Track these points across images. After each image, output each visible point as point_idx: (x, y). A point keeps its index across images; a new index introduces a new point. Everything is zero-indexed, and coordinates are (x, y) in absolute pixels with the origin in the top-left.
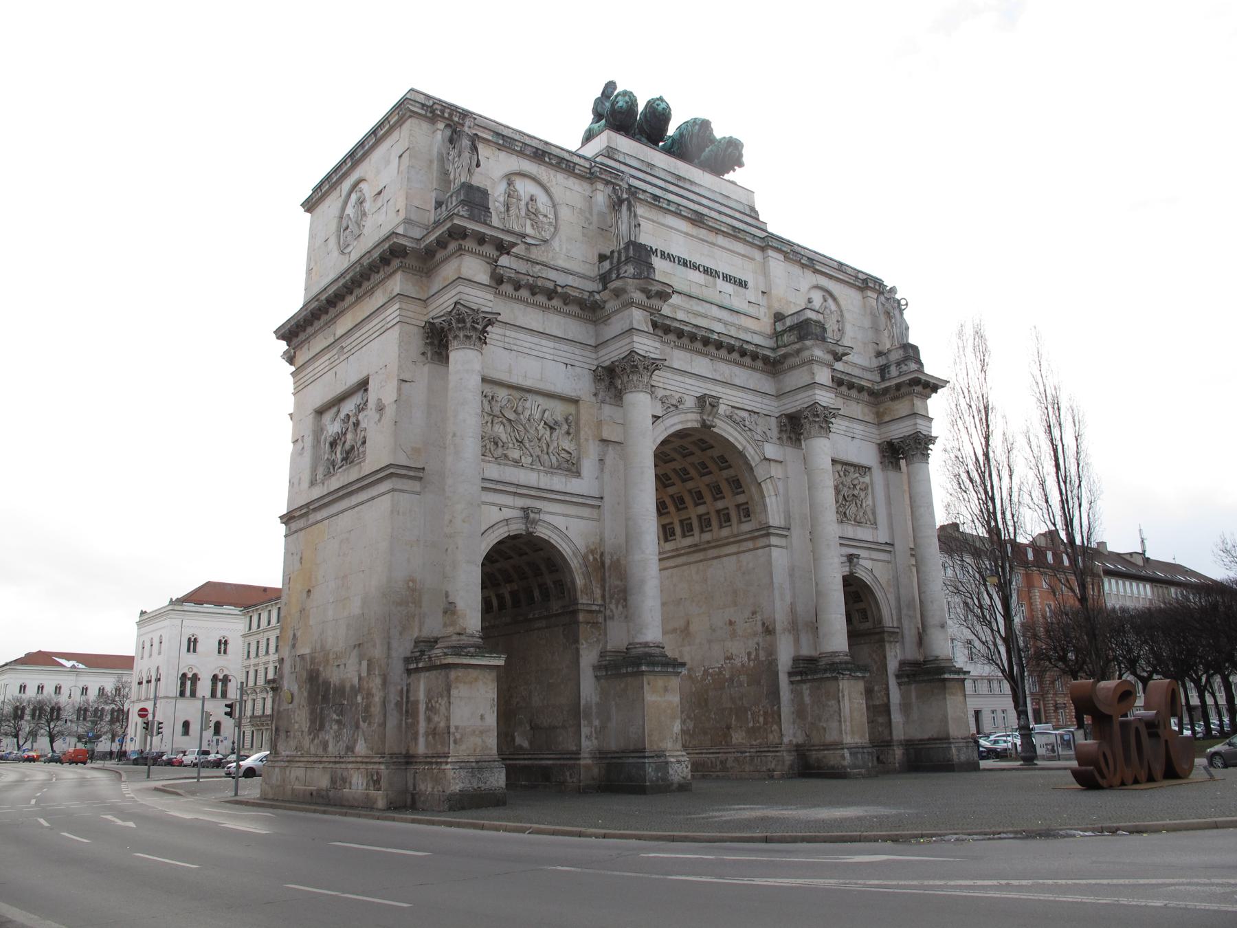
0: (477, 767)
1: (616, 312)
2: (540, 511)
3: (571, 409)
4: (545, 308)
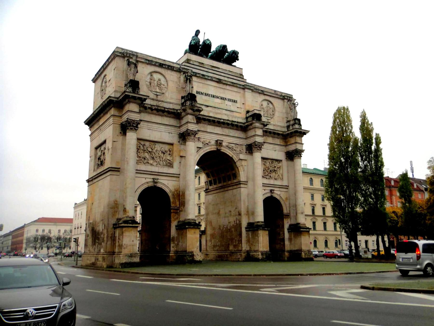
0: (131, 256)
1: (185, 116)
2: (158, 179)
3: (171, 147)
4: (162, 116)
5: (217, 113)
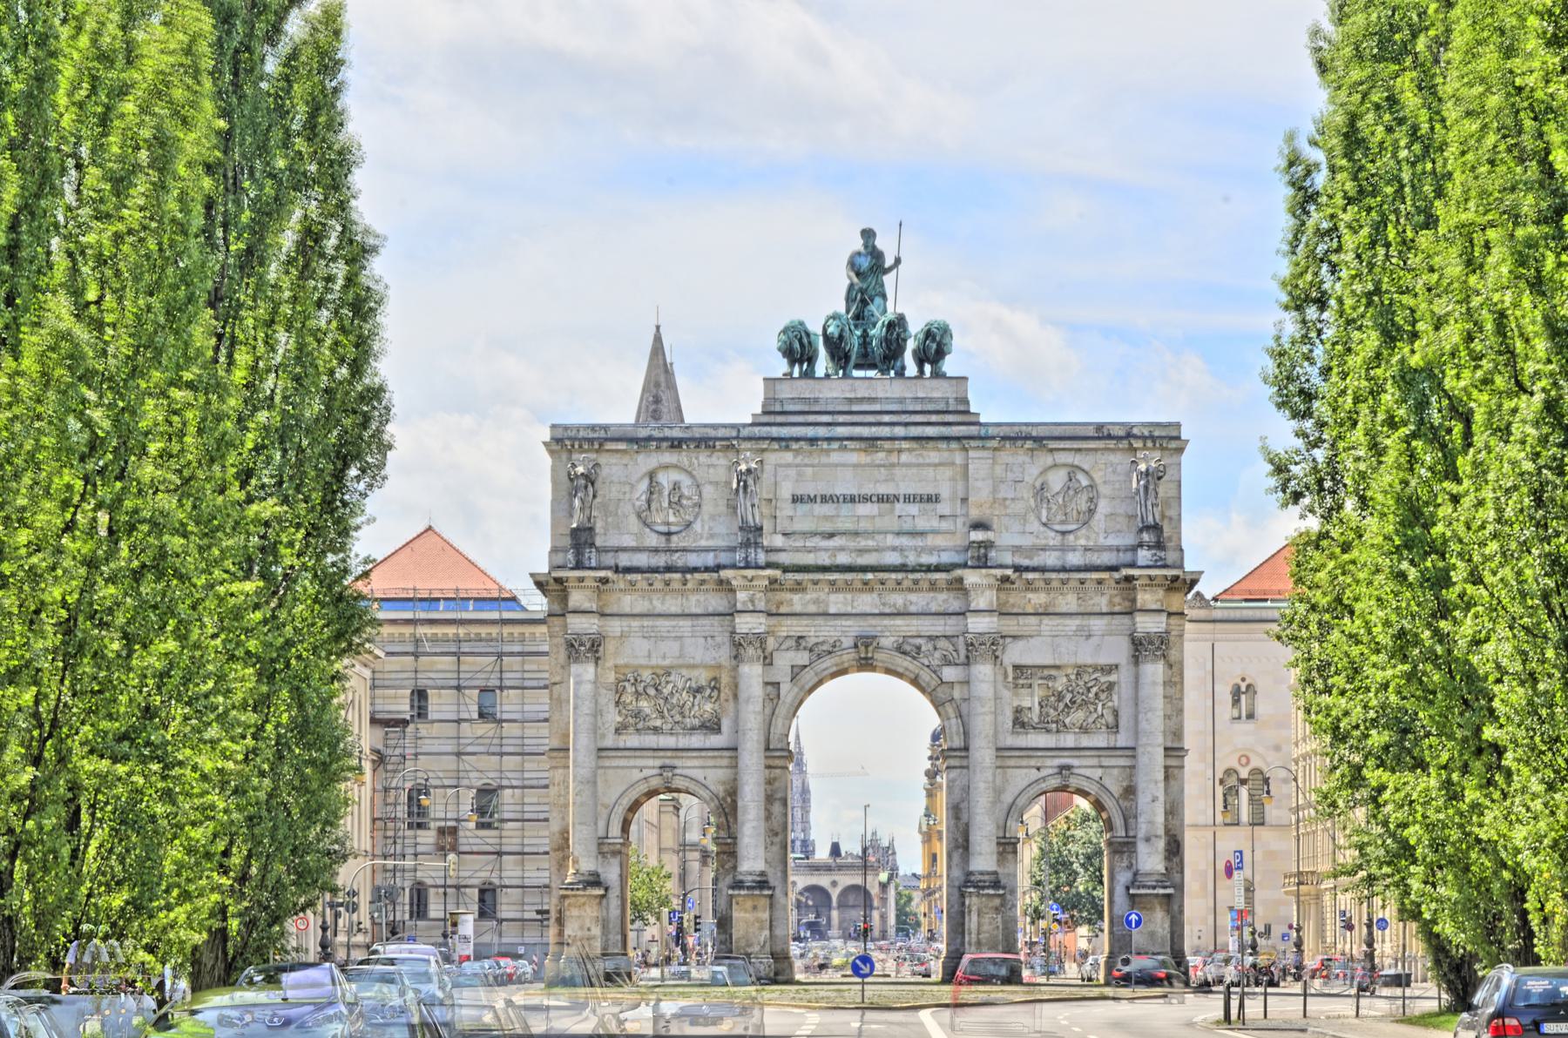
5: (861, 551)
